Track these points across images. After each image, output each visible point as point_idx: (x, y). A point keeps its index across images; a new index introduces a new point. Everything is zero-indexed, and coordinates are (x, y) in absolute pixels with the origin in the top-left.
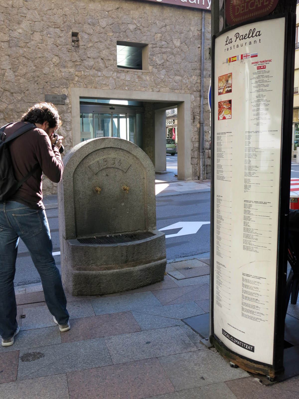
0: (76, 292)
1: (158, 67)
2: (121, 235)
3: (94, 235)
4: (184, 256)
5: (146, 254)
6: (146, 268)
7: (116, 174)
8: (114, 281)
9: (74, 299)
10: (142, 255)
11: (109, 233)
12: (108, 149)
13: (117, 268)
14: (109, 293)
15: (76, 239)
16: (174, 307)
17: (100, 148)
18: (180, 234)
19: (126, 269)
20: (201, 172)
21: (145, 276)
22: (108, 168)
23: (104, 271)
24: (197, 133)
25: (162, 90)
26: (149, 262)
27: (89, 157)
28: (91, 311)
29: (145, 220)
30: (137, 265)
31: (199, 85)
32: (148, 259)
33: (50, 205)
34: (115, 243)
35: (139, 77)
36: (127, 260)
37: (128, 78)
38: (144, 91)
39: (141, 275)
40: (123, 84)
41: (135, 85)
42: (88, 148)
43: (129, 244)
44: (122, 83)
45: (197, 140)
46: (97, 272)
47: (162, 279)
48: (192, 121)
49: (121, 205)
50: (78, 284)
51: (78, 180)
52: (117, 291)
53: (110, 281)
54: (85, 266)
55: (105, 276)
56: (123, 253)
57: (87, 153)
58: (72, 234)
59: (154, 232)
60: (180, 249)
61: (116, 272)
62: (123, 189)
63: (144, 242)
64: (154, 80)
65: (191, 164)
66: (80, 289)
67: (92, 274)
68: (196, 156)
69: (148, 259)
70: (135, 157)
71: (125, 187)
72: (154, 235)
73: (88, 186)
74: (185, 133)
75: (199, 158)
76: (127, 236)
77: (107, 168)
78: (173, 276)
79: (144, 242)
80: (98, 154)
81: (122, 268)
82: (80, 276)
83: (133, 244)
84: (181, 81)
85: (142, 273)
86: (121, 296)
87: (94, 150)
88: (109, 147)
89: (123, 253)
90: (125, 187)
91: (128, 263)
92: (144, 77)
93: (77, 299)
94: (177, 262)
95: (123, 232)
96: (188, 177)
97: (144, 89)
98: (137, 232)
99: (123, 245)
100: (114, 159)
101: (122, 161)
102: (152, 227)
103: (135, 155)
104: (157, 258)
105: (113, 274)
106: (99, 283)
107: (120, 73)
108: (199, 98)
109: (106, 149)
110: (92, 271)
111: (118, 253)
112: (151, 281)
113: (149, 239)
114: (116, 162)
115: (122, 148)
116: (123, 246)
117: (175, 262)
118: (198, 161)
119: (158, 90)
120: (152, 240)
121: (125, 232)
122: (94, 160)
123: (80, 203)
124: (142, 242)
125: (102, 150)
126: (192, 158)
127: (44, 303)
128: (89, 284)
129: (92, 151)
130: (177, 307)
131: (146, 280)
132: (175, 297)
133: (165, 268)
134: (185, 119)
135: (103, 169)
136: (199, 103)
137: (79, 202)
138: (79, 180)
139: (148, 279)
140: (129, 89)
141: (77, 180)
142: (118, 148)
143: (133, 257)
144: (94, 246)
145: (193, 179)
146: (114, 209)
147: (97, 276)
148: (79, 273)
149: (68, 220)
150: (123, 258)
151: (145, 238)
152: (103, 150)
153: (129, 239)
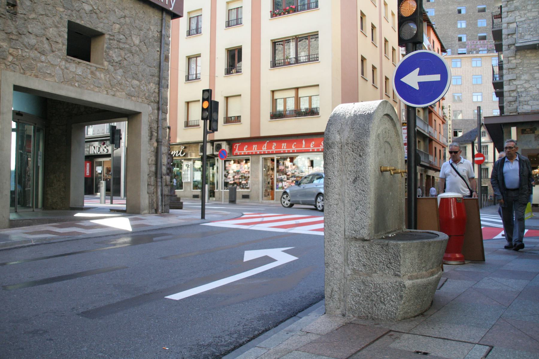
1: (114, 64)
20: (160, 203)
24: (154, 153)
25: (118, 94)
31: (157, 95)
35: (92, 73)
37: (79, 71)
38: (97, 92)
40: (73, 77)
41: (88, 82)
44: (71, 76)
45: (154, 162)
48: (149, 138)
64: (110, 81)
65: (148, 193)
68: (152, 183)
74: (142, 153)
75: (156, 186)
84: (139, 87)
92: (98, 74)
96: (144, 210)
97: (97, 89)
107: (70, 62)
108: (156, 111)
118: (155, 189)
119: (113, 94)
126: (148, 185)
134: (142, 134)
136: (156, 117)
140: (79, 86)
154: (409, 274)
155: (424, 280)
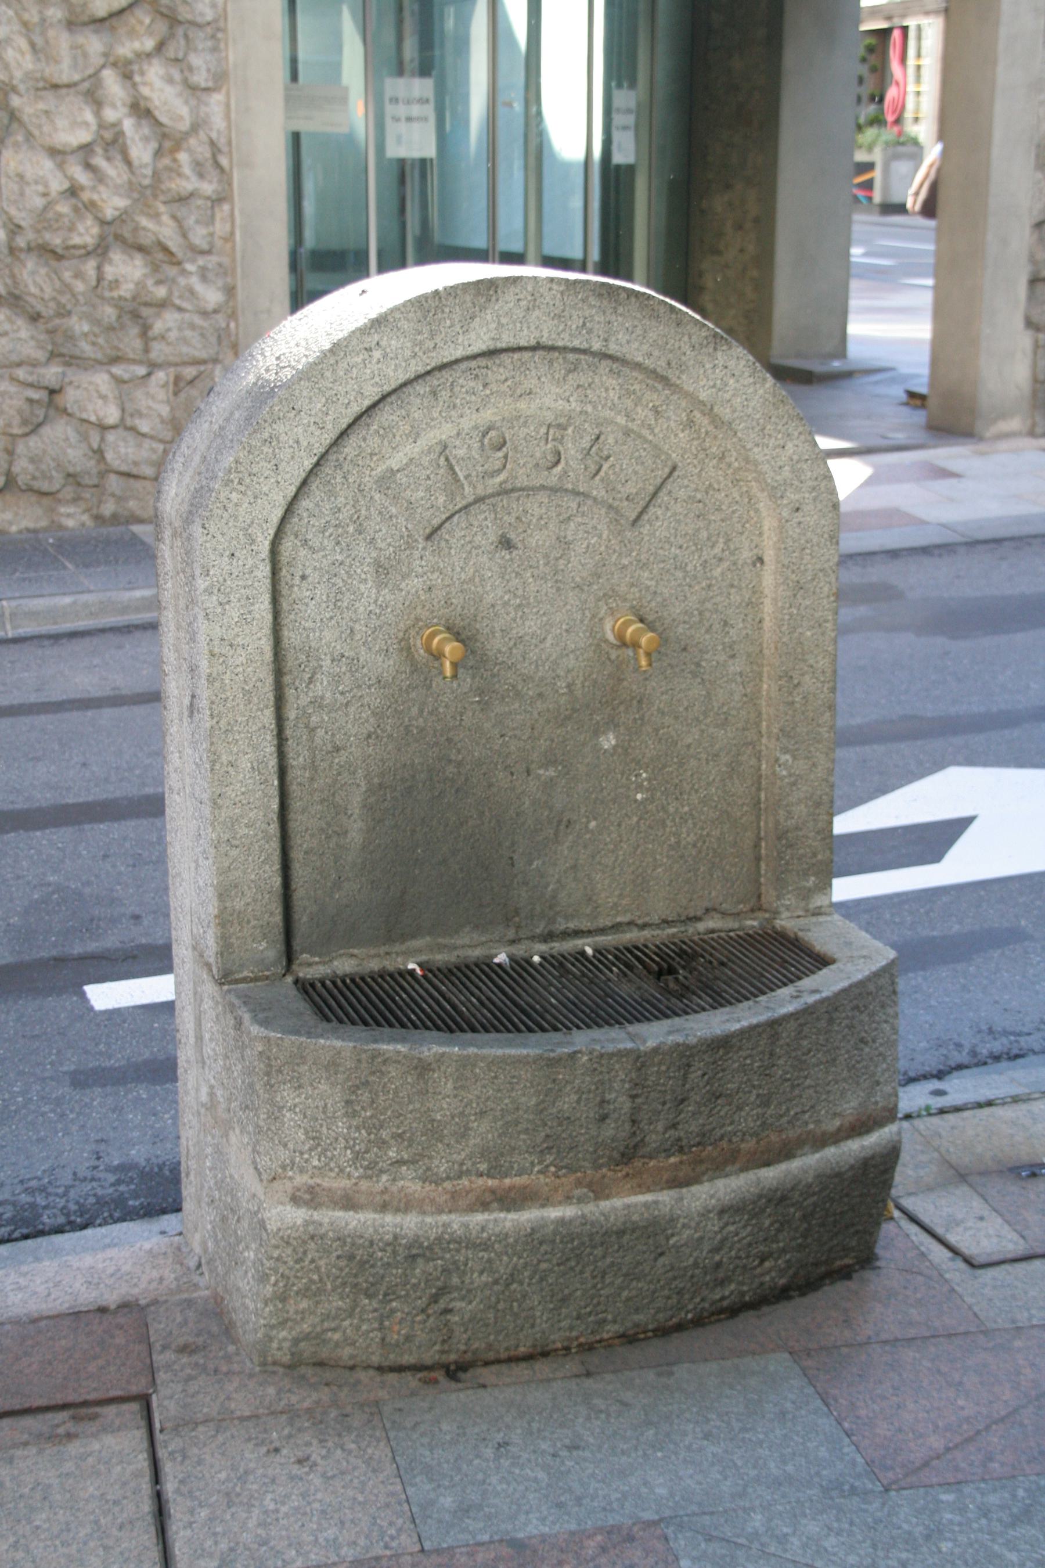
0: (286, 1345)
2: (589, 951)
3: (408, 954)
4: (997, 1046)
5: (766, 1104)
6: (760, 1196)
7: (570, 538)
8: (542, 1279)
9: (271, 1390)
10: (740, 1108)
11: (511, 934)
12: (516, 356)
13: (568, 1199)
14: (503, 1355)
15: (289, 979)
16: (963, 1510)
17: (459, 353)
18: (959, 866)
19: (626, 1203)
21: (750, 1245)
22: (513, 490)
23: (480, 1218)
26: (786, 1152)
27: (386, 416)
28: (388, 1505)
29: (757, 846)
30: (703, 1174)
32: (774, 1137)
33: (86, 605)
34: (556, 1029)
36: (635, 1147)
39: (724, 1240)
42: (377, 354)
43: (651, 1044)
46: (429, 1220)
47: (867, 1260)
49: (596, 748)
50: (297, 1293)
51: (303, 577)
52: (559, 1345)
53: (512, 1278)
54: (349, 1176)
55: (485, 1246)
56: (608, 1097)
57: (372, 394)
58: (264, 944)
59: (820, 936)
60: (964, 988)
61: (562, 1222)
62: (611, 637)
63: (753, 1028)
66: (314, 1326)
67: (396, 1237)
69: (774, 1137)
70: (709, 411)
71: (627, 624)
72: (823, 961)
73: (374, 622)
74: (1000, 108)
76: (630, 958)
77: (504, 491)
78: (940, 1231)
79: (757, 1026)
80: (445, 394)
81: (599, 1191)
82: (312, 1245)
83: (680, 1039)
85: (731, 1228)
86: (589, 1383)
87: (417, 367)
88: (523, 343)
89: (608, 1102)
90: (627, 624)
91: (638, 1163)
93: (294, 1399)
94: (957, 1109)
95: (602, 931)
96: (1003, 416)
98: (701, 927)
99: (610, 1048)
101: (611, 440)
102: (806, 895)
103: (703, 396)
104: (837, 1123)
105: (533, 1239)
106: (443, 1290)
109: (504, 357)
110: (398, 1210)
111: (578, 1101)
112: (791, 1272)
113: (784, 1002)
114: (571, 450)
115: (613, 348)
116: (612, 1055)
117: (942, 1111)
120: (808, 1011)
121: (616, 927)
122: (418, 434)
123: (320, 732)
124: (745, 1023)
125: (473, 364)
127: (63, 1415)
128: (369, 1296)
129: (402, 378)
130: (985, 1512)
131: (758, 1271)
132: (967, 1420)
133: (887, 1184)
135: (479, 500)
137: (313, 730)
138: (313, 577)
139: (767, 1264)
141: (297, 580)
142: (584, 352)
143: (674, 1126)
144: (415, 1053)
145: (1034, 425)
146: (551, 772)
147: (430, 1248)
148: (307, 1223)
149: (234, 853)
150: (609, 1131)
151: (761, 987)
152: (482, 362)
153: (651, 989)
154: (301, 1180)
155: (410, 1223)
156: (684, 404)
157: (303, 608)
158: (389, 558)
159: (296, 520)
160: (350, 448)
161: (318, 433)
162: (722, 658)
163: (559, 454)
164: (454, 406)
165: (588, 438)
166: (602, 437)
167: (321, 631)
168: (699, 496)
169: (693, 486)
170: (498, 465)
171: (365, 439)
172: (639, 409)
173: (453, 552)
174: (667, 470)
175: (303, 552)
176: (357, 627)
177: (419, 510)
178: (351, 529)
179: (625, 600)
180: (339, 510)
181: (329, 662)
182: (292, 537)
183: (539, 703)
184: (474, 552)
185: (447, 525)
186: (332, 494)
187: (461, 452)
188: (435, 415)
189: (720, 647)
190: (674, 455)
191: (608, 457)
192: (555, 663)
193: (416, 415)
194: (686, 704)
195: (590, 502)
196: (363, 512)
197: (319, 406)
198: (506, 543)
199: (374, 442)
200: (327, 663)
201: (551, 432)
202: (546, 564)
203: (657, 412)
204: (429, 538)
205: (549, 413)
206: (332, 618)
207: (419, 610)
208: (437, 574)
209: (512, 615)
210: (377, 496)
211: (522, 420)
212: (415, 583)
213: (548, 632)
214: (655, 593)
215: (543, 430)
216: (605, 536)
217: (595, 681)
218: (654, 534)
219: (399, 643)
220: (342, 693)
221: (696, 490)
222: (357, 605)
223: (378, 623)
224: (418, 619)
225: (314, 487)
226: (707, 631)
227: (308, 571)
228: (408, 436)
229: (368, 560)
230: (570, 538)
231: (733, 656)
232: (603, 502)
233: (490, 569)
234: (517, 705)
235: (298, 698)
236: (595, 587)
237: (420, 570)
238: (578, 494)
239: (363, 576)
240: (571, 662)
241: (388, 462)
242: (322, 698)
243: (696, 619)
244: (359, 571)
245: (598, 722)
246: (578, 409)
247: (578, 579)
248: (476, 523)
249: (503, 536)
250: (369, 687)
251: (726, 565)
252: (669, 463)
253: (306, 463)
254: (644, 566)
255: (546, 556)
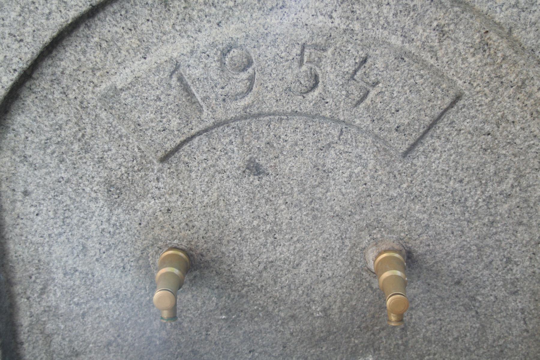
7: (329, 166)
51: (26, 193)
73: (107, 239)
77: (247, 115)
100: (316, 46)
103: (500, 17)
114: (330, 75)
123: (57, 339)
138: (37, 194)
141: (19, 196)
156: (477, 24)
157: (29, 223)
158: (121, 178)
159: (11, 135)
160: (68, 59)
161: (16, 46)
162: (501, 294)
163: (316, 77)
164: (191, 19)
165: (352, 62)
166: (369, 61)
167: (50, 246)
168: (488, 128)
169: (481, 117)
170: (241, 87)
171: (84, 52)
172: (419, 29)
173: (193, 175)
174: (448, 100)
175: (23, 169)
176: (89, 244)
177: (149, 133)
178: (76, 147)
179: (392, 232)
180: (61, 128)
181: (61, 275)
182: (9, 153)
183: (291, 324)
184: (218, 176)
185: (186, 147)
186: (50, 110)
187: (197, 72)
188: (168, 28)
189: (500, 283)
190: (460, 82)
191: (375, 84)
192: (310, 287)
193: (144, 28)
194: (456, 334)
195: (354, 130)
196: (88, 130)
197: (13, 15)
198: (254, 169)
199: (95, 56)
200: (59, 276)
201: (307, 52)
202: (300, 192)
203: (443, 33)
204: (164, 159)
205: (305, 31)
206: (60, 234)
207: (157, 230)
208: (175, 197)
209: (262, 240)
210: (103, 115)
211: (269, 39)
212: (150, 205)
213: (302, 259)
214: (427, 226)
215: (296, 50)
216: (370, 166)
217: (354, 308)
218: (430, 166)
219: (138, 260)
220: (77, 304)
221: (485, 122)
222: (88, 222)
223: (113, 241)
224: (156, 240)
225: (29, 101)
226: (486, 267)
227: (31, 188)
228: (136, 51)
229: (97, 179)
230: (329, 166)
231: (515, 293)
232: (369, 132)
233: (236, 194)
234: (267, 325)
235: (31, 306)
236: (357, 217)
237: (157, 192)
238: (338, 121)
239: (93, 195)
240: (328, 288)
241: (113, 79)
242: (57, 307)
243: (475, 254)
244: (88, 189)
245: (356, 345)
246: (343, 27)
247: (337, 208)
248: (220, 147)
249: (250, 161)
250: (107, 300)
251: (514, 202)
252: (452, 93)
253: (5, 79)
254: (416, 199)
255: (301, 183)
